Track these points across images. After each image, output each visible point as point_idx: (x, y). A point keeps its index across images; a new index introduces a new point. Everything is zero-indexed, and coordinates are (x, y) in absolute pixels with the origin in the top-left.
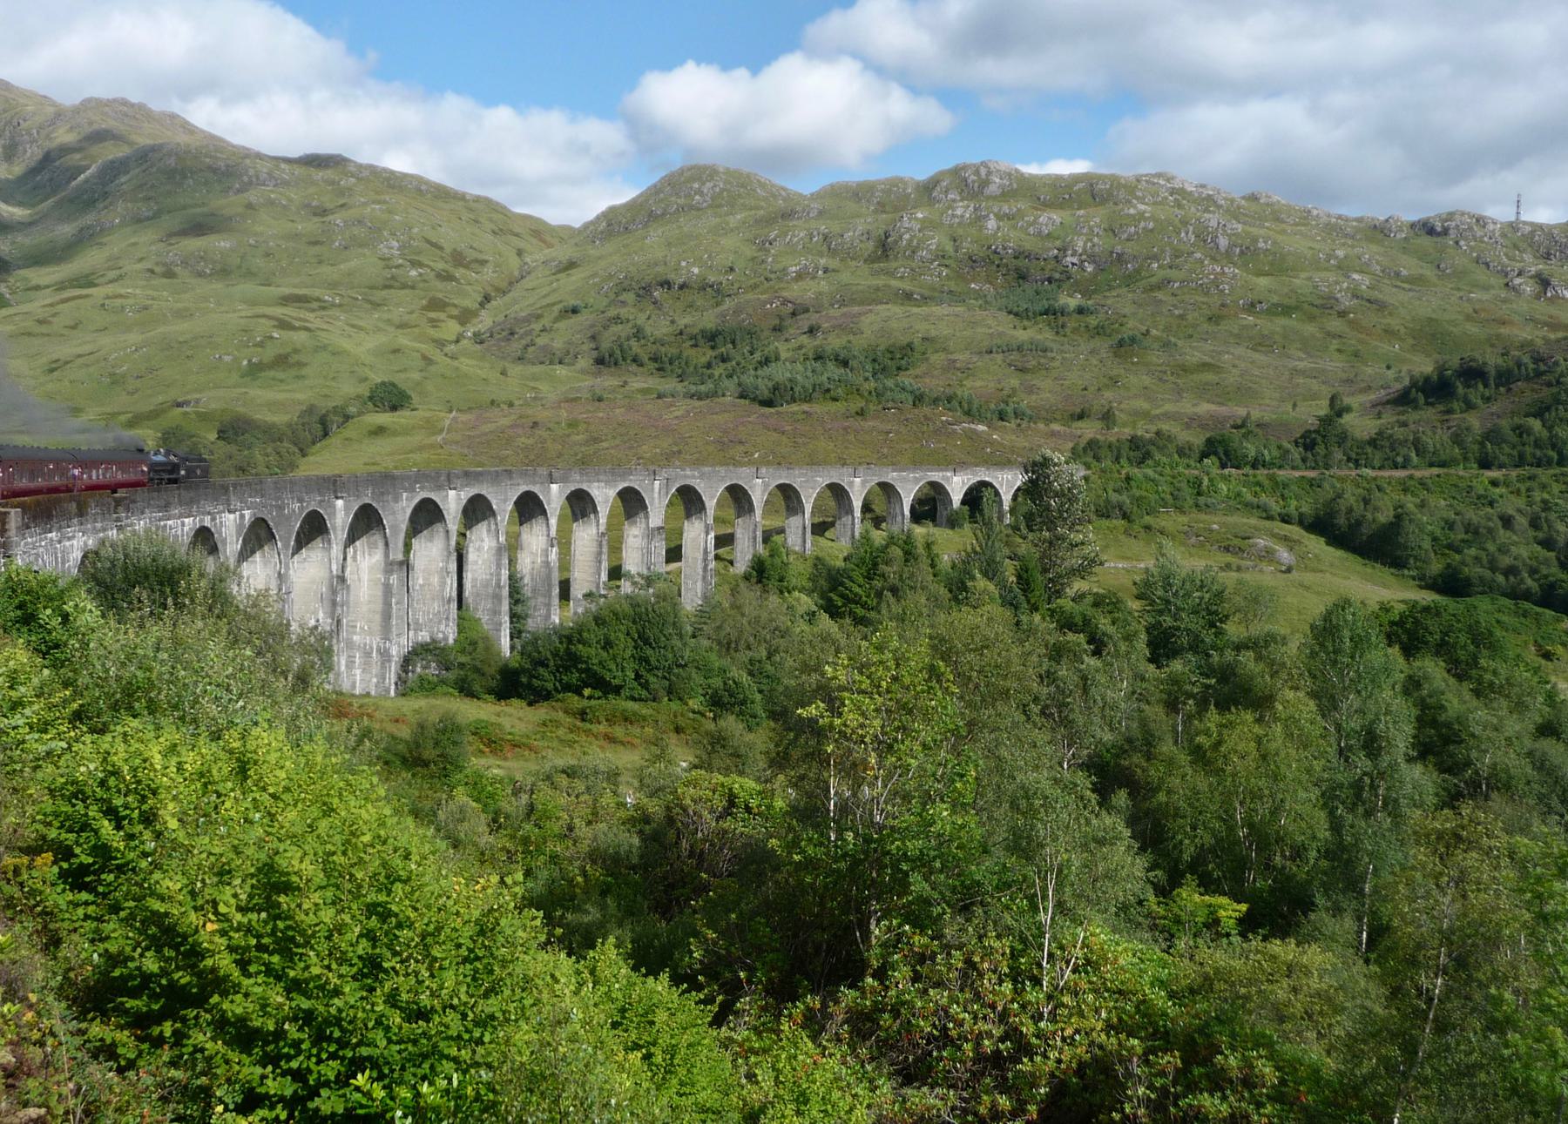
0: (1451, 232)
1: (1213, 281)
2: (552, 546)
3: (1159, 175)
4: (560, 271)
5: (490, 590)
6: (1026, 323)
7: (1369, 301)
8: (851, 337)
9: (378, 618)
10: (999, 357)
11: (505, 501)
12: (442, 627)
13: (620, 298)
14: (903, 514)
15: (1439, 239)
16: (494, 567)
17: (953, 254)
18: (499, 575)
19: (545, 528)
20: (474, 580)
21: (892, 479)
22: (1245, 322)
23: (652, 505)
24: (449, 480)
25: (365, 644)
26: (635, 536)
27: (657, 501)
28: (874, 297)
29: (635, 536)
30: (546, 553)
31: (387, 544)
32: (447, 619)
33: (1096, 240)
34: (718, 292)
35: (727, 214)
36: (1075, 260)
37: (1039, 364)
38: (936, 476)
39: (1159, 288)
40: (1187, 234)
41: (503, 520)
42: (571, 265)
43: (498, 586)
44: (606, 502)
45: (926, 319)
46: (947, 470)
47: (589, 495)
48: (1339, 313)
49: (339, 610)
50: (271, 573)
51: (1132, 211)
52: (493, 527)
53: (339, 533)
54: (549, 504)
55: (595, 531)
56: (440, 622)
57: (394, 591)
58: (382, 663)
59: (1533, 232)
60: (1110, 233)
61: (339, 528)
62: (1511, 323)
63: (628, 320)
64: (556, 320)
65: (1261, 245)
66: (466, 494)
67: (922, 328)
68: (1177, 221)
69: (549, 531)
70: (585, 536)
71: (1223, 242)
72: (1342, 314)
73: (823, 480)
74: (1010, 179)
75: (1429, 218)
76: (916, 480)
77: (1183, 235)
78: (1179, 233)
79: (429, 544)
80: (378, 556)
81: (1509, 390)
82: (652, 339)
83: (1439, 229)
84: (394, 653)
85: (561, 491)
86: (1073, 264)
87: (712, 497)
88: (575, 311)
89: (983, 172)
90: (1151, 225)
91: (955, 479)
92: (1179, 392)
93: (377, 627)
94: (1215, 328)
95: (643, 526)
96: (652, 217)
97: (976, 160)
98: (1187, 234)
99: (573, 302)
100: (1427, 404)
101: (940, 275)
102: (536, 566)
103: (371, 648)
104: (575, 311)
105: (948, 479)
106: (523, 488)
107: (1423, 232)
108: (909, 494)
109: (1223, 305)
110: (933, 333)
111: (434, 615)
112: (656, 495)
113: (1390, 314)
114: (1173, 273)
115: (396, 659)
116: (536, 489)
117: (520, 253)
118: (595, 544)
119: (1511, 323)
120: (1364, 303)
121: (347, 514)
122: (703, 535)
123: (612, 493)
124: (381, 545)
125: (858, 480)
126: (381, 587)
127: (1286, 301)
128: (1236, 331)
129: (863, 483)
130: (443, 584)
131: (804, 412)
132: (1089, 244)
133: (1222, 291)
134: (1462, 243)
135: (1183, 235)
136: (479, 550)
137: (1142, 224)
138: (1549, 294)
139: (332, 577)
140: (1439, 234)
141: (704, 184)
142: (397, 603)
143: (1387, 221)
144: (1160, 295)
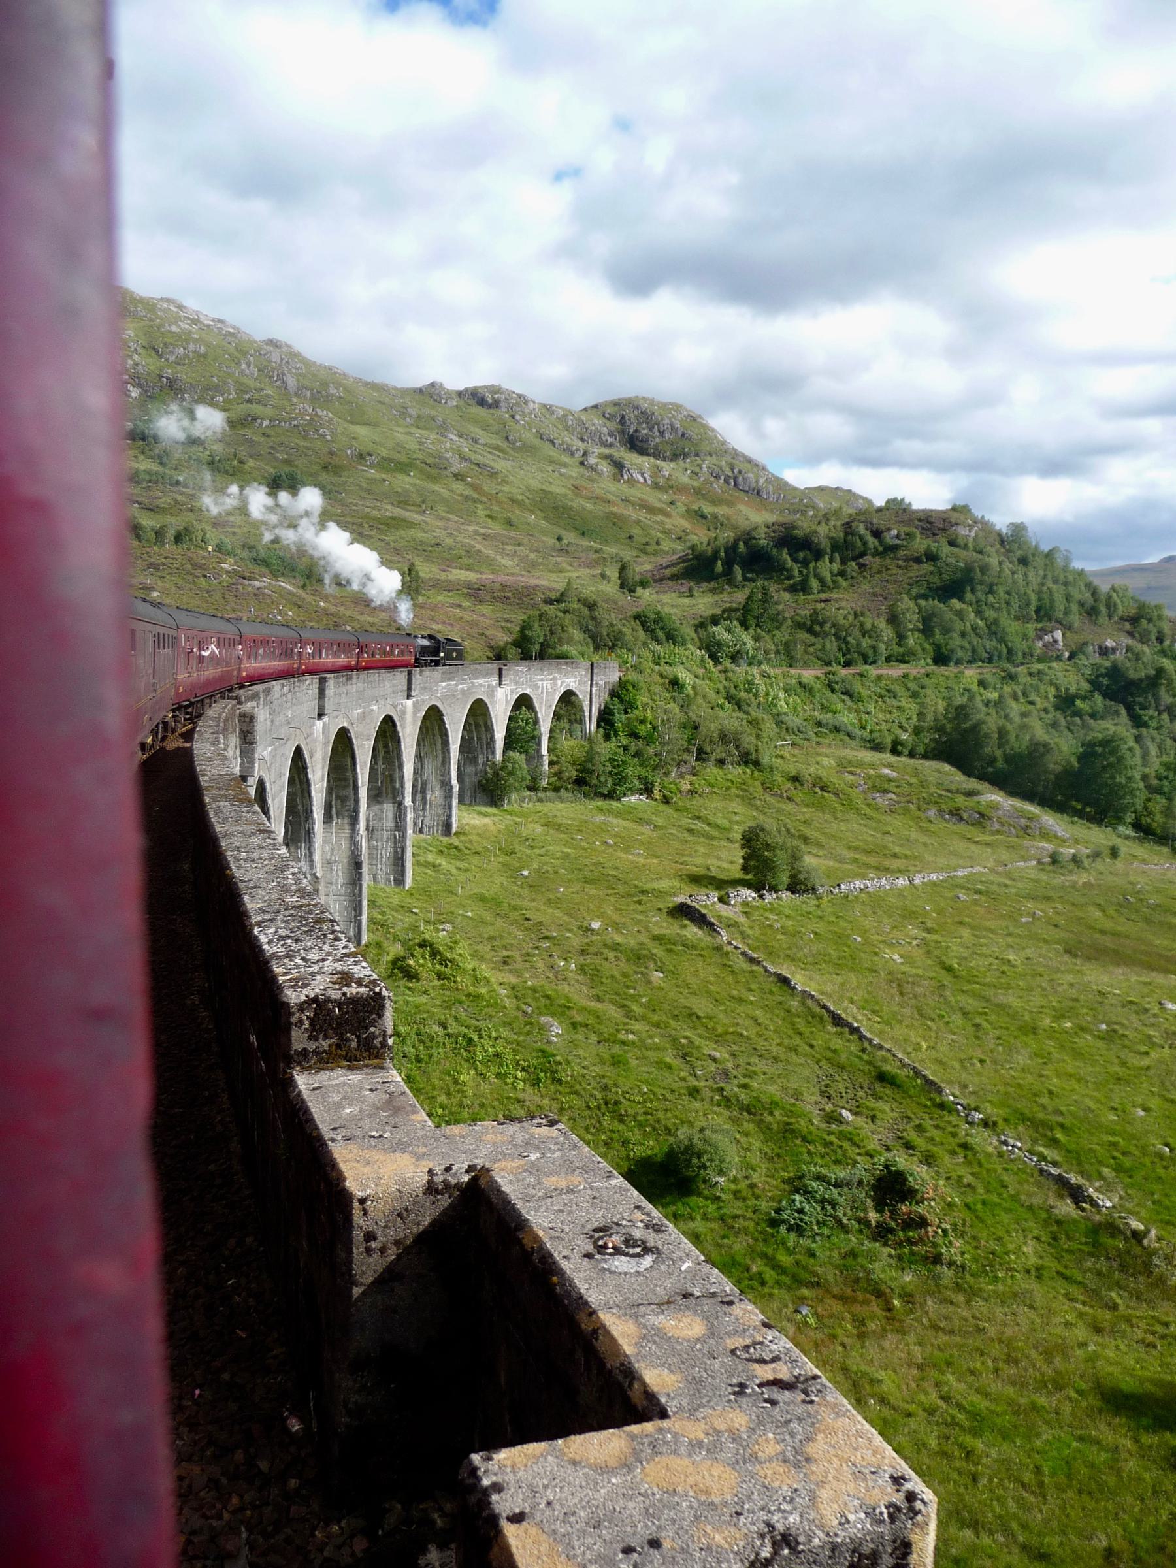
0: (503, 404)
1: (310, 422)
3: (168, 300)
7: (478, 464)
14: (446, 785)
15: (492, 411)
22: (369, 476)
33: (136, 357)
37: (177, 502)
40: (249, 366)
46: (487, 674)
48: (455, 475)
51: (174, 329)
59: (565, 416)
60: (153, 354)
62: (614, 504)
65: (332, 391)
68: (232, 349)
71: (291, 382)
72: (458, 477)
75: (476, 388)
77: (244, 366)
78: (238, 363)
81: (862, 566)
83: (490, 401)
90: (203, 349)
91: (501, 693)
94: (335, 479)
98: (249, 366)
100: (745, 579)
105: (491, 692)
107: (473, 402)
108: (457, 731)
109: (331, 453)
113: (505, 482)
114: (257, 409)
119: (614, 504)
120: (473, 467)
125: (410, 703)
127: (397, 456)
128: (364, 485)
132: (130, 362)
133: (324, 436)
134: (518, 417)
135: (244, 366)
137: (191, 347)
138: (626, 477)
140: (490, 406)
143: (433, 385)
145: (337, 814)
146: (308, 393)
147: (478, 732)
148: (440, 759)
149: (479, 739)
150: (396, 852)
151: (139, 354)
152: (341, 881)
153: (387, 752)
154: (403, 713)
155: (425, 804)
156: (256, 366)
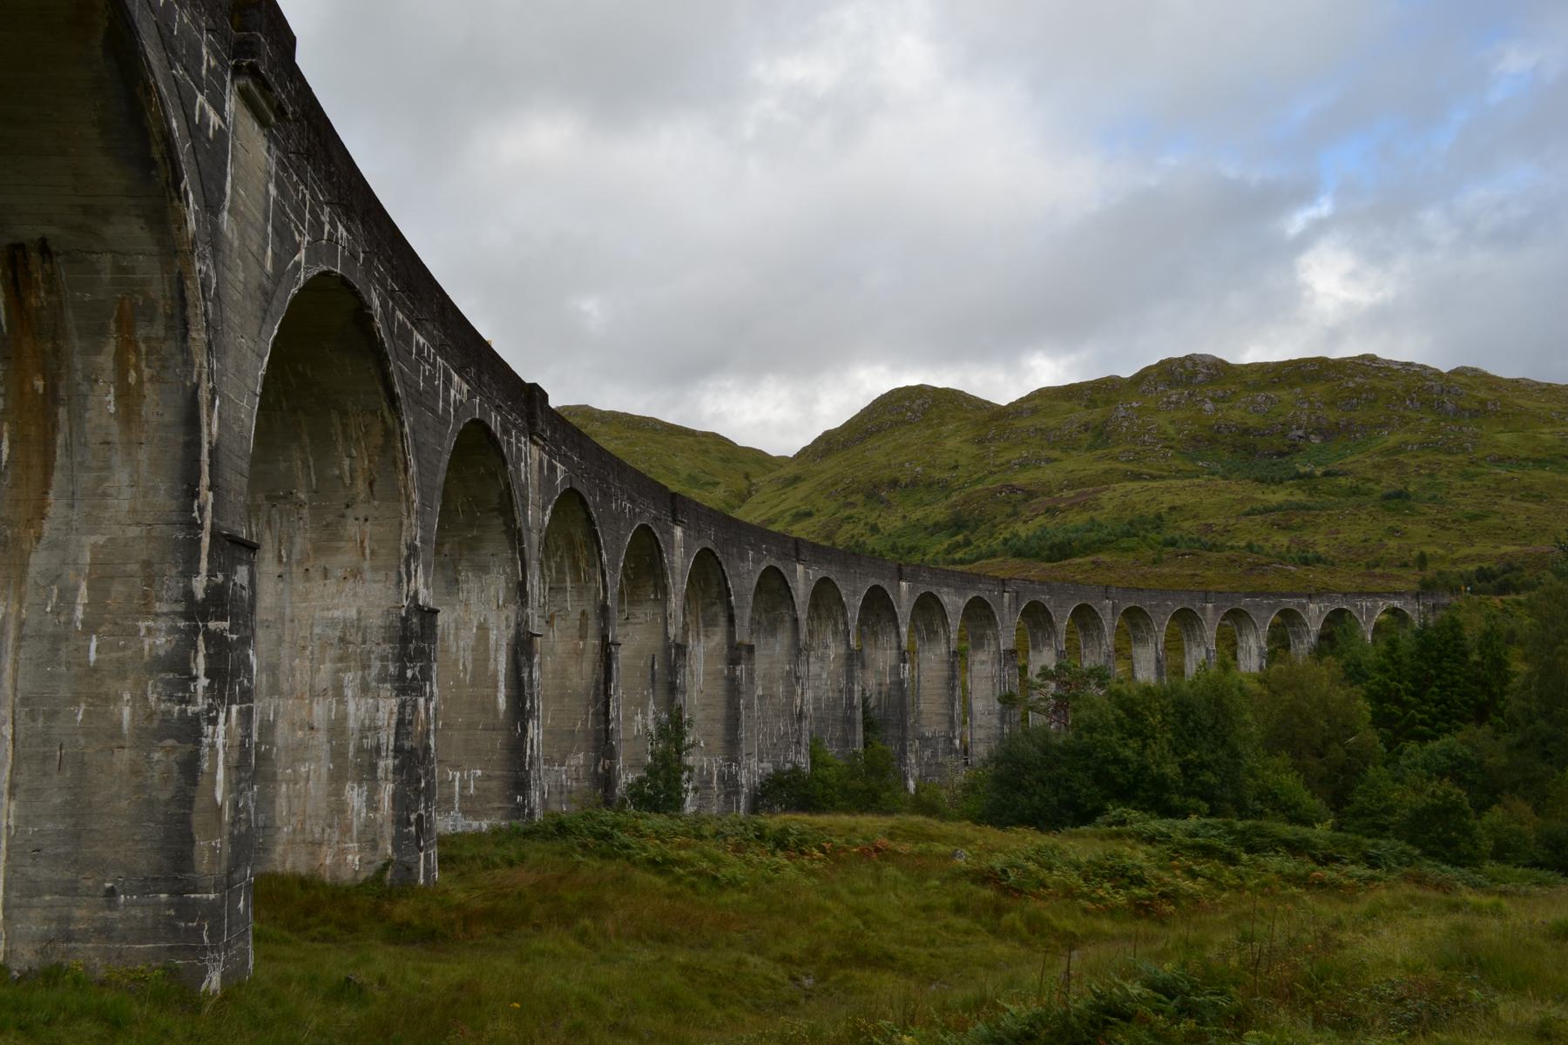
2: (905, 662)
3: (1363, 357)
4: (788, 485)
5: (839, 713)
6: (1273, 488)
8: (1092, 513)
9: (719, 728)
10: (1258, 518)
12: (791, 756)
13: (849, 500)
16: (843, 682)
17: (1175, 436)
18: (851, 691)
19: (893, 635)
20: (817, 699)
23: (1002, 620)
24: (797, 550)
25: (702, 768)
26: (983, 663)
27: (1007, 618)
28: (1105, 479)
29: (983, 663)
30: (896, 670)
31: (731, 620)
32: (798, 743)
34: (946, 487)
35: (940, 425)
36: (1300, 433)
38: (1291, 603)
39: (1399, 452)
41: (853, 618)
42: (796, 479)
43: (851, 706)
44: (956, 613)
45: (1167, 490)
47: (938, 601)
49: (679, 699)
50: (589, 609)
52: (841, 627)
53: (678, 578)
54: (899, 607)
55: (944, 650)
56: (787, 749)
57: (743, 688)
58: (727, 795)
61: (678, 571)
63: (860, 520)
64: (790, 524)
66: (816, 573)
67: (1168, 500)
69: (899, 642)
70: (932, 661)
73: (1174, 606)
74: (1217, 370)
76: (1271, 608)
77: (1408, 402)
79: (771, 640)
80: (718, 637)
82: (886, 534)
84: (744, 781)
85: (911, 590)
86: (1300, 437)
87: (1062, 621)
88: (809, 515)
89: (1189, 364)
92: (1469, 540)
93: (718, 743)
95: (993, 649)
96: (870, 433)
97: (1182, 355)
98: (1412, 401)
99: (803, 508)
101: (1165, 456)
102: (884, 689)
103: (710, 774)
104: (809, 515)
105: (1304, 607)
106: (873, 581)
108: (1265, 624)
110: (1178, 503)
111: (780, 738)
112: (1006, 610)
115: (745, 790)
116: (884, 584)
117: (747, 476)
118: (945, 665)
121: (687, 554)
123: (962, 603)
124: (722, 621)
126: (722, 682)
129: (1216, 609)
130: (791, 694)
131: (1094, 562)
132: (1313, 417)
135: (1408, 402)
136: (822, 659)
139: (667, 649)
141: (914, 402)
142: (746, 708)
144: (1401, 457)
146: (1467, 414)
151: (1322, 410)
154: (1203, 609)
156: (1418, 401)
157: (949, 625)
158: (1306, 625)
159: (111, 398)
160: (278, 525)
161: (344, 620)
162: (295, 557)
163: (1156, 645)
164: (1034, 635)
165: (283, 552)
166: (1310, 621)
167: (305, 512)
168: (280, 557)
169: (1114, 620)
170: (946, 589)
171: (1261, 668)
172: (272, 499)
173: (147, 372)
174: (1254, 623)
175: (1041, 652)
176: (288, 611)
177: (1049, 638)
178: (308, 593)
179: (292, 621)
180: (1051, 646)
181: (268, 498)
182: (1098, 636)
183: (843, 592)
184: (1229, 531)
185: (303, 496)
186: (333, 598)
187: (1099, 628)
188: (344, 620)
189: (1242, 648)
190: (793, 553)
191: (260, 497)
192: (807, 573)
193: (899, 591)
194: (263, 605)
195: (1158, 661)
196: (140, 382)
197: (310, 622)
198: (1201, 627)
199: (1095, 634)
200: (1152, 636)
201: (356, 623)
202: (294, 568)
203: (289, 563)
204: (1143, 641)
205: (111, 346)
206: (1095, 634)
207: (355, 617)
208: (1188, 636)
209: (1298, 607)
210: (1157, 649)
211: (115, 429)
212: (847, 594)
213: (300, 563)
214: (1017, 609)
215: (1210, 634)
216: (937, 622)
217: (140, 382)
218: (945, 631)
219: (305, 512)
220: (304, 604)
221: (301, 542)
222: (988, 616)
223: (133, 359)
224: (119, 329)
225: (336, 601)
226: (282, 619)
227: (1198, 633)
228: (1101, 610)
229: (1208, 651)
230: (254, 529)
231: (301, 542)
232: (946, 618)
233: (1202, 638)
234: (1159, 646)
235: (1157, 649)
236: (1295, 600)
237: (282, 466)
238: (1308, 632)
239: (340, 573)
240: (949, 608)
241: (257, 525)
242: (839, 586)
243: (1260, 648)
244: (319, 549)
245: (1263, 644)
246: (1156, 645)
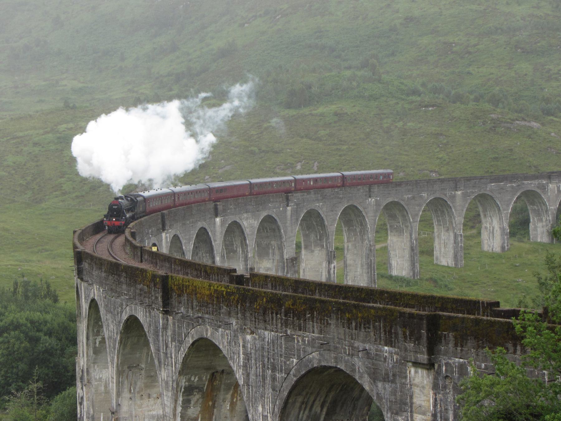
11: (189, 240)
21: (491, 191)
23: (285, 232)
27: (289, 229)
38: (531, 185)
54: (215, 241)
73: (426, 196)
95: (277, 257)
105: (544, 188)
106: (200, 225)
108: (508, 206)
122: (325, 264)
123: (256, 224)
125: (459, 193)
129: (465, 195)
131: (336, 114)
145: (406, 232)
147: (541, 206)
148: (498, 217)
149: (542, 209)
150: (455, 253)
152: (407, 256)
153: (448, 212)
154: (453, 197)
155: (493, 237)
157: (246, 245)
158: (545, 204)
159: (228, 405)
160: (131, 377)
161: (158, 415)
162: (137, 390)
163: (411, 235)
164: (306, 236)
165: (132, 388)
166: (549, 201)
167: (143, 372)
168: (130, 390)
169: (375, 216)
170: (245, 215)
171: (503, 248)
172: (130, 368)
173: (239, 398)
174: (498, 206)
175: (312, 251)
176: (134, 413)
177: (320, 240)
178: (142, 405)
179: (136, 417)
180: (322, 246)
181: (128, 368)
182: (360, 232)
183: (183, 242)
184: (470, 53)
185: (143, 366)
186: (152, 406)
187: (362, 225)
188: (158, 415)
189: (486, 228)
190: (161, 226)
191: (125, 367)
192: (166, 238)
193: (215, 227)
194: (123, 410)
195: (412, 249)
196: (237, 401)
197: (143, 417)
198: (451, 215)
199: (358, 230)
200: (407, 227)
201: (162, 416)
202: (136, 395)
203: (134, 393)
204: (399, 231)
205: (231, 392)
206: (358, 230)
207: (162, 414)
208: (438, 221)
209: (538, 187)
210: (411, 238)
211: (228, 414)
212: (185, 243)
213: (138, 392)
214: (297, 220)
215: (459, 219)
216: (237, 243)
217: (237, 401)
218: (243, 251)
219: (143, 372)
220: (140, 410)
221: (140, 384)
222: (274, 230)
223: (236, 395)
224: (234, 388)
225: (154, 407)
226: (131, 416)
227: (447, 219)
228: (364, 208)
229: (456, 236)
230: (121, 380)
231: (140, 384)
232: (245, 240)
233: (451, 223)
234: (413, 236)
235: (411, 238)
236: (536, 182)
237: (138, 355)
238: (547, 211)
239: (155, 396)
240: (247, 231)
241: (122, 378)
242: (181, 239)
243: (503, 229)
244: (147, 386)
245: (506, 225)
246: (411, 235)
